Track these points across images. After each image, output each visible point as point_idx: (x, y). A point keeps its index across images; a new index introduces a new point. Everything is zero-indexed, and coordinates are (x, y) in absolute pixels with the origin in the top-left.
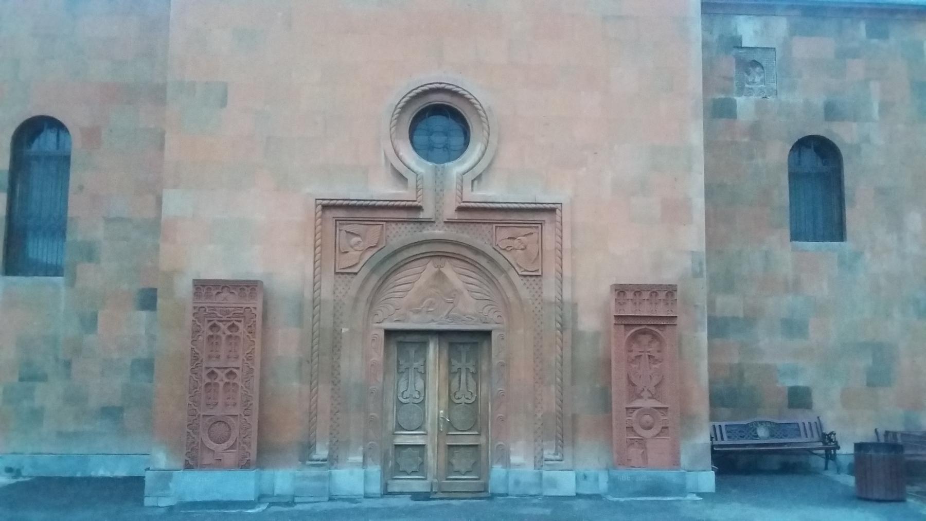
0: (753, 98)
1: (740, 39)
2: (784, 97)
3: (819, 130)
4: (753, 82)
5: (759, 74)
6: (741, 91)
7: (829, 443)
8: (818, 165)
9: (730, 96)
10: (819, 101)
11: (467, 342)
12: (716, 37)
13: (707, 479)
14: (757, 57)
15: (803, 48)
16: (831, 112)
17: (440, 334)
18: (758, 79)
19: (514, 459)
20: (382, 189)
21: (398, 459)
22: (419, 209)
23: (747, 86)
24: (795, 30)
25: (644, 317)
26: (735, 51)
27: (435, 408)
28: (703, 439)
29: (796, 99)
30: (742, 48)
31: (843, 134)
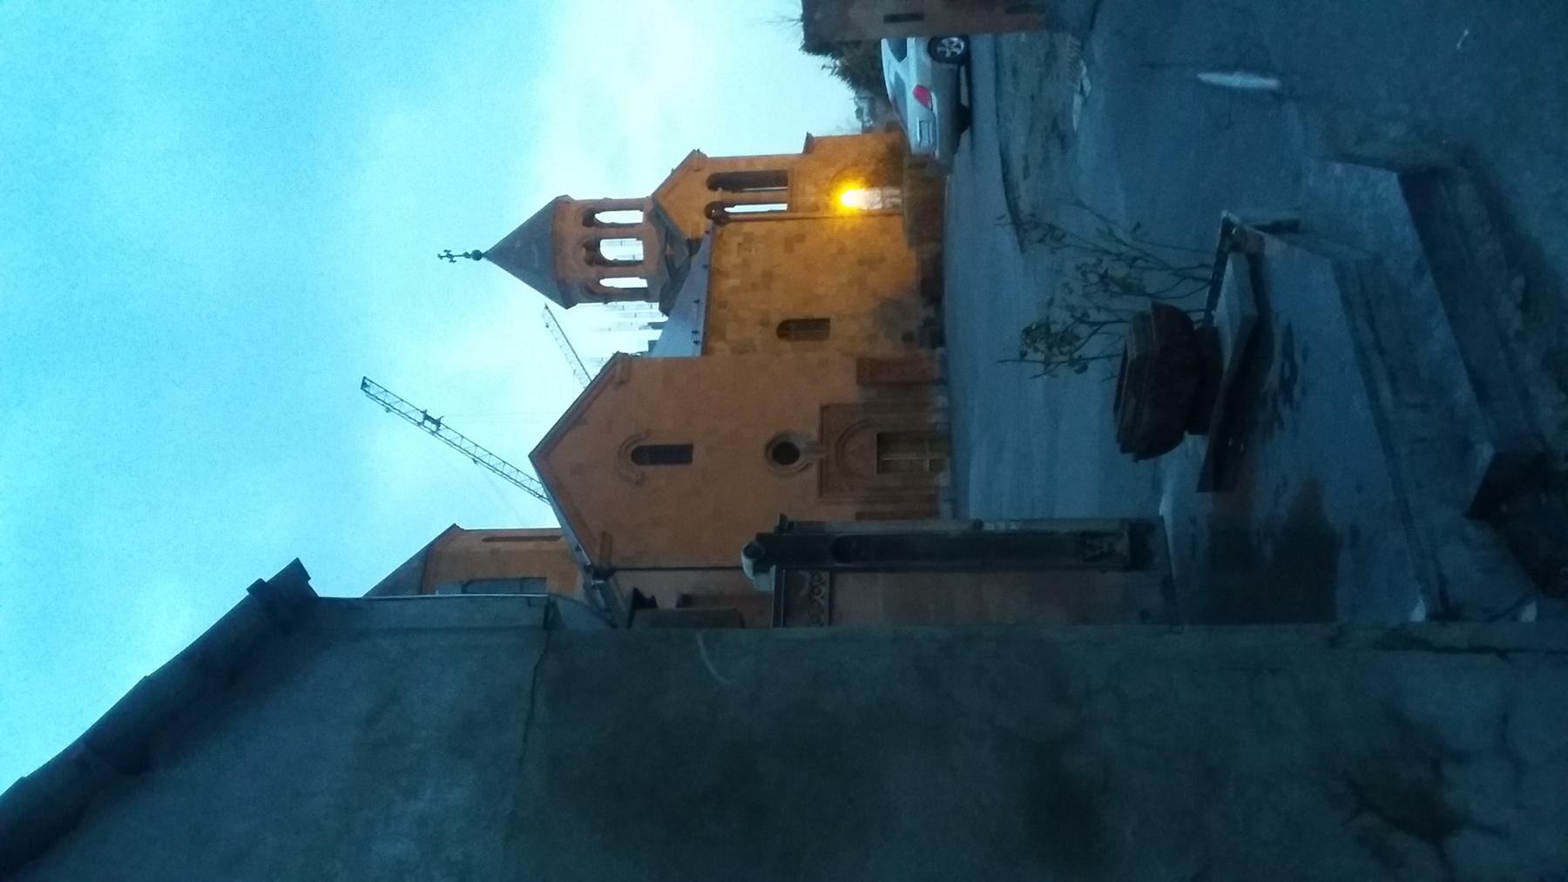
3: (774, 330)
7: (928, 322)
8: (788, 329)
11: (884, 442)
13: (940, 350)
15: (731, 335)
16: (765, 323)
17: (879, 455)
19: (933, 420)
20: (814, 470)
21: (936, 467)
22: (821, 462)
25: (869, 371)
27: (912, 456)
28: (923, 352)
31: (776, 319)
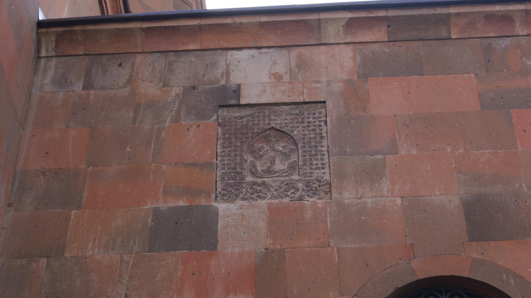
0: (263, 203)
1: (237, 91)
2: (348, 196)
4: (269, 172)
5: (286, 156)
6: (233, 190)
9: (203, 202)
10: (447, 198)
12: (176, 90)
14: (277, 122)
18: (280, 166)
23: (249, 179)
24: (370, 68)
26: (224, 113)
29: (386, 196)
30: (239, 106)
